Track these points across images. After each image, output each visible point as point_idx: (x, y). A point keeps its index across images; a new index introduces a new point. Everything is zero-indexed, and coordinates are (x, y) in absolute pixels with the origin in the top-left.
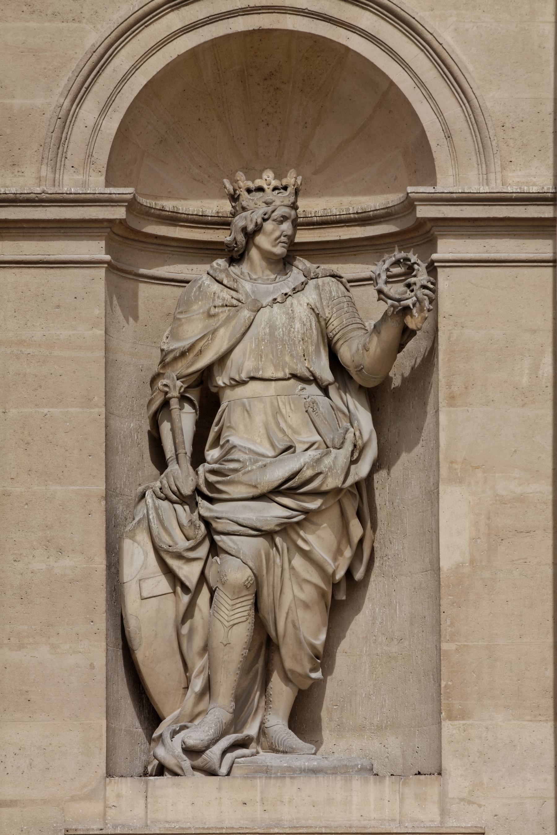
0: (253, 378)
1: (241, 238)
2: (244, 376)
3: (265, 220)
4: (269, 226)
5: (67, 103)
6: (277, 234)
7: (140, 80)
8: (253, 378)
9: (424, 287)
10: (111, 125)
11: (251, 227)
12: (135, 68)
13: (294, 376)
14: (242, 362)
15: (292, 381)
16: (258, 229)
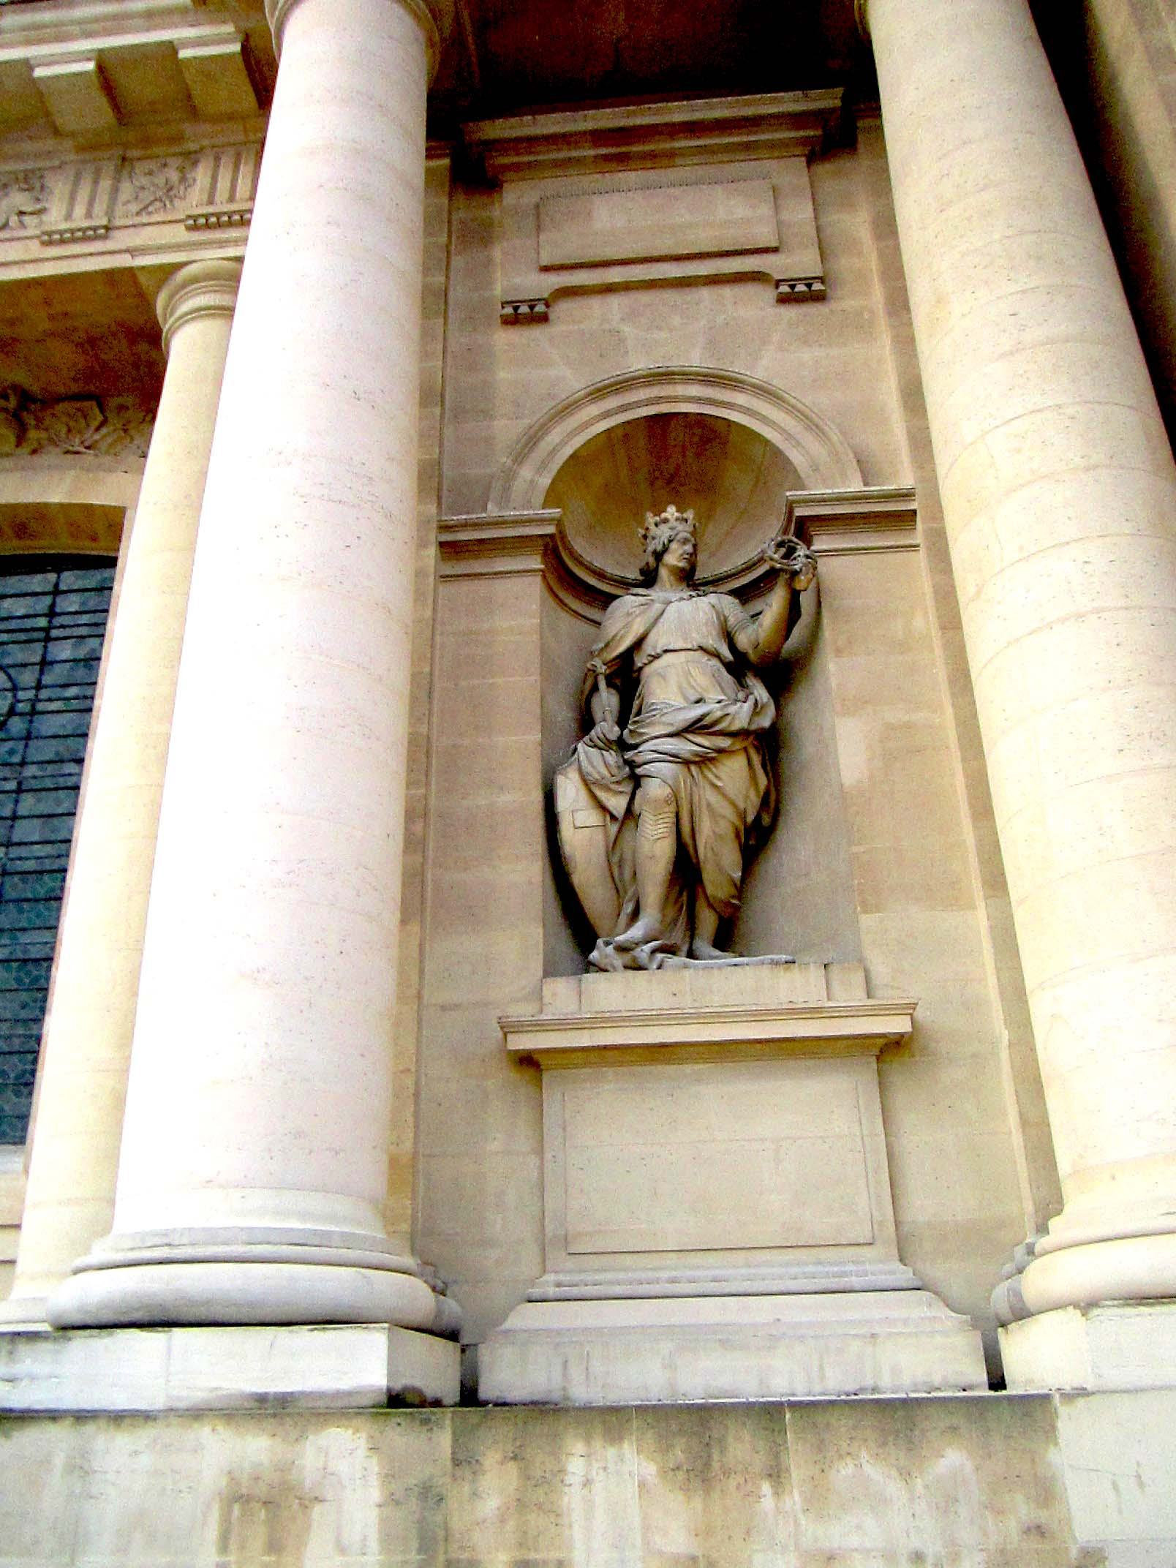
0: (666, 651)
1: (651, 560)
2: (659, 651)
3: (670, 541)
4: (674, 546)
5: (509, 462)
6: (680, 552)
7: (568, 451)
8: (666, 651)
9: (807, 557)
10: (545, 481)
11: (659, 548)
12: (564, 443)
13: (701, 648)
14: (657, 641)
15: (699, 653)
16: (665, 549)
